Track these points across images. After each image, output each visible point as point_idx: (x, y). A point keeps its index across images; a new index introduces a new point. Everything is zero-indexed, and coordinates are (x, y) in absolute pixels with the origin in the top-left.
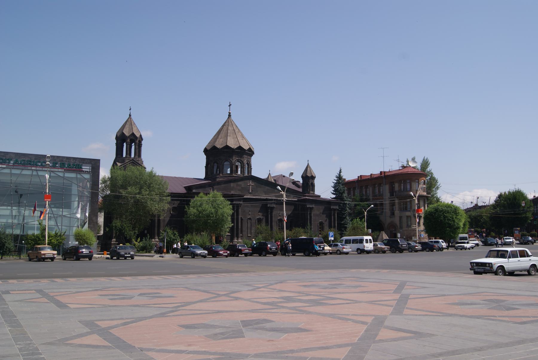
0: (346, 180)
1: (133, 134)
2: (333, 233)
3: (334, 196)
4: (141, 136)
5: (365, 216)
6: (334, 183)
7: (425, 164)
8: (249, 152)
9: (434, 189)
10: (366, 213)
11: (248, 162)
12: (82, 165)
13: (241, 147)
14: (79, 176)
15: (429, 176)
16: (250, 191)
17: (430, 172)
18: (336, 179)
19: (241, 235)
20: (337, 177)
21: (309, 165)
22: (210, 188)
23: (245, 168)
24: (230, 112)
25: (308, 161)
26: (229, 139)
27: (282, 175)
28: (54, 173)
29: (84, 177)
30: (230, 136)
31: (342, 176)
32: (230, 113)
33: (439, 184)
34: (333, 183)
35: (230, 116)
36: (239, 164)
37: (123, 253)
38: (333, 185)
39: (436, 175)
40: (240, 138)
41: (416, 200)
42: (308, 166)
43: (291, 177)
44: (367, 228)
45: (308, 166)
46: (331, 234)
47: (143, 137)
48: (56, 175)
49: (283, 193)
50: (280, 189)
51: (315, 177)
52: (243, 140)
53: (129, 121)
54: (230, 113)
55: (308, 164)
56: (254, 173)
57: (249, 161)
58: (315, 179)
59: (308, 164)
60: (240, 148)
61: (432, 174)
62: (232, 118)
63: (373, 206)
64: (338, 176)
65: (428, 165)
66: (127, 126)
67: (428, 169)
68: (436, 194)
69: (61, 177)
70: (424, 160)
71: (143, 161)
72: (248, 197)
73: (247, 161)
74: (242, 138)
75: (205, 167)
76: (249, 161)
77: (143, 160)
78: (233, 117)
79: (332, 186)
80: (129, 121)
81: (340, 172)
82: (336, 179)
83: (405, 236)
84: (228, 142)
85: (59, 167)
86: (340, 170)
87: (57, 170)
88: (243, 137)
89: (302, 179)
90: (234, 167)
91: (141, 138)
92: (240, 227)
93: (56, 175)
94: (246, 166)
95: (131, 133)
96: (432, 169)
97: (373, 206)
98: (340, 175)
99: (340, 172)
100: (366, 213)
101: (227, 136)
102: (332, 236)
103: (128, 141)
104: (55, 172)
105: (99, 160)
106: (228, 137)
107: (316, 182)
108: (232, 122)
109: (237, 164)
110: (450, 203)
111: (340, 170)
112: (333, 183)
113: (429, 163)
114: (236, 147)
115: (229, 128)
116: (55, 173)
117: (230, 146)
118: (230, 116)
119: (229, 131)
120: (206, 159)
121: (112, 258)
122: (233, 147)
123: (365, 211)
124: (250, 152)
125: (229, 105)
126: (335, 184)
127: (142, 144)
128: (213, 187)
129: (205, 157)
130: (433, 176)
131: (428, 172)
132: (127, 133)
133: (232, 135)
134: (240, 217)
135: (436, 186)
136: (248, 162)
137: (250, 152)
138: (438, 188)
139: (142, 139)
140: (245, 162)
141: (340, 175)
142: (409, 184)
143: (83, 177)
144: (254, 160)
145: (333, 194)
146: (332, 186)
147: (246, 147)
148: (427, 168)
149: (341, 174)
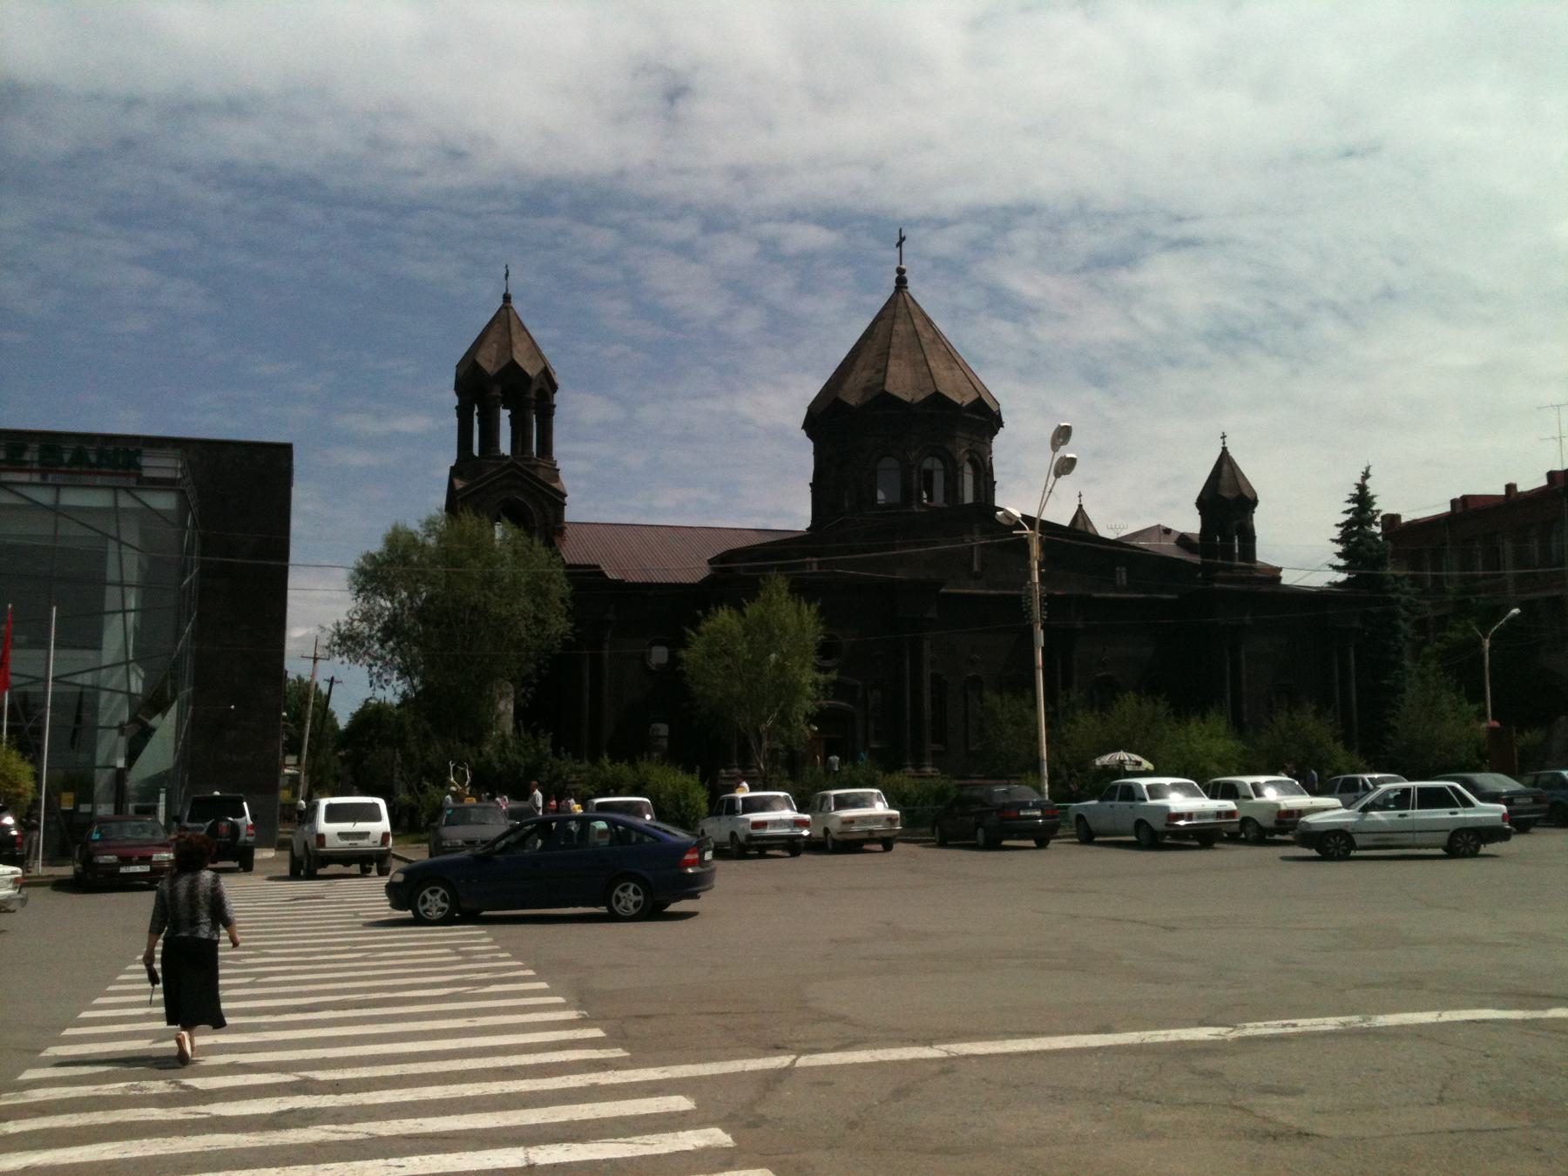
0: (1404, 520)
1: (513, 366)
3: (1341, 577)
4: (546, 373)
10: (1487, 643)
11: (976, 456)
14: (125, 501)
16: (976, 568)
19: (938, 747)
21: (1227, 453)
23: (960, 478)
24: (903, 266)
25: (1224, 437)
26: (894, 367)
27: (1159, 526)
28: (12, 491)
29: (148, 506)
30: (899, 357)
32: (901, 271)
35: (901, 282)
36: (938, 464)
37: (112, 858)
38: (1336, 533)
40: (938, 366)
42: (1225, 459)
43: (1062, 448)
45: (1225, 459)
47: (558, 379)
48: (28, 503)
49: (1028, 531)
52: (952, 368)
53: (504, 321)
54: (901, 271)
55: (1224, 449)
57: (980, 456)
58: (1257, 509)
59: (1224, 449)
60: (938, 401)
62: (909, 290)
63: (1516, 611)
66: (492, 336)
71: (558, 470)
72: (967, 591)
75: (811, 484)
76: (980, 456)
77: (557, 467)
78: (913, 287)
80: (504, 321)
84: (889, 381)
85: (36, 466)
87: (24, 477)
89: (1198, 511)
90: (915, 477)
91: (548, 384)
93: (22, 502)
94: (968, 469)
95: (504, 362)
97: (1516, 611)
98: (1362, 488)
101: (885, 355)
103: (494, 393)
104: (11, 487)
105: (285, 451)
106: (889, 362)
107: (1262, 521)
108: (911, 305)
109: (927, 464)
114: (921, 397)
115: (896, 328)
117: (896, 393)
118: (901, 282)
119: (894, 340)
120: (814, 453)
122: (907, 398)
123: (1485, 637)
125: (898, 240)
127: (554, 406)
132: (489, 362)
134: (927, 672)
136: (976, 456)
139: (554, 388)
140: (962, 454)
141: (1362, 488)
145: (1337, 568)
147: (964, 398)
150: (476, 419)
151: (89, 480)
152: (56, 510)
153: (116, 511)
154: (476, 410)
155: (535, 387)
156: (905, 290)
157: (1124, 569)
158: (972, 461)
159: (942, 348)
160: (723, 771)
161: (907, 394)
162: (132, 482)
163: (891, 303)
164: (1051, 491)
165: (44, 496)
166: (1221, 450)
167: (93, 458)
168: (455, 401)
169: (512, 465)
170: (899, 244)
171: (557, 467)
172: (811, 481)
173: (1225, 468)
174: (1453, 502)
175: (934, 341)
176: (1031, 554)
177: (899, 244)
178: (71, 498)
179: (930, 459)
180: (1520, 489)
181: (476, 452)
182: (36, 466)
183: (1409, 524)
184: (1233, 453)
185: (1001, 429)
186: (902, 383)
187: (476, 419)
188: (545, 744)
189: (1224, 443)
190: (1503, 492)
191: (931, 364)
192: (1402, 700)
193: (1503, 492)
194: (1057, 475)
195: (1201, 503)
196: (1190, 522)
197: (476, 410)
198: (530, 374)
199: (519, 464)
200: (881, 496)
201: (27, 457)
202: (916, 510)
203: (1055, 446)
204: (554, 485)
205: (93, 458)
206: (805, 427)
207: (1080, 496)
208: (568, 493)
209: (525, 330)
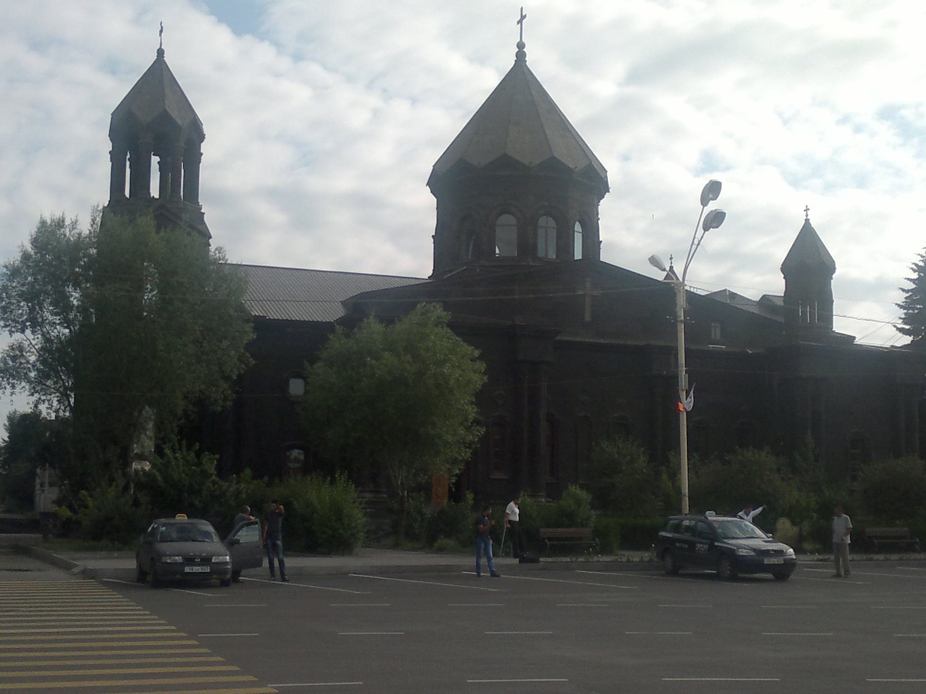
3: (907, 340)
6: (907, 291)
13: (559, 162)
18: (915, 276)
25: (807, 210)
32: (521, 46)
34: (903, 290)
35: (521, 56)
36: (552, 223)
54: (521, 46)
55: (807, 220)
59: (807, 220)
71: (204, 213)
77: (202, 211)
79: (899, 305)
82: (915, 276)
112: (903, 290)
125: (519, 18)
139: (202, 137)
145: (901, 330)
146: (899, 305)
150: (128, 163)
154: (128, 156)
164: (699, 244)
166: (804, 222)
170: (520, 22)
171: (202, 211)
172: (434, 234)
176: (678, 302)
177: (520, 22)
181: (127, 194)
185: (607, 194)
187: (128, 163)
188: (210, 464)
189: (807, 216)
194: (706, 228)
196: (776, 285)
197: (128, 156)
198: (180, 122)
200: (497, 251)
203: (704, 201)
204: (199, 227)
207: (671, 259)
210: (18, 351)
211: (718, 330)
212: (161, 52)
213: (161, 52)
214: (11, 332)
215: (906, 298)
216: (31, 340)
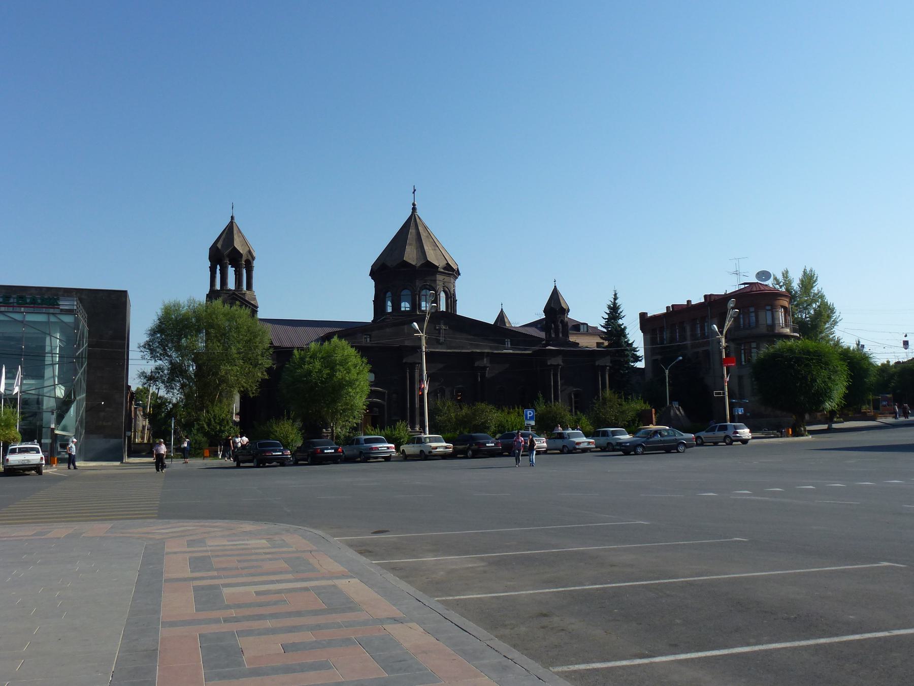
2: (532, 411)
4: (250, 252)
5: (665, 377)
6: (605, 319)
7: (808, 281)
8: (447, 272)
9: (827, 326)
10: (667, 372)
11: (446, 289)
12: (58, 299)
13: (429, 261)
14: (53, 319)
15: (818, 302)
17: (820, 294)
20: (609, 307)
22: (366, 336)
28: (4, 314)
30: (411, 244)
31: (619, 306)
32: (414, 205)
33: (837, 314)
34: (604, 318)
35: (414, 209)
39: (830, 299)
40: (428, 248)
41: (723, 340)
44: (671, 400)
46: (530, 414)
47: (255, 254)
48: (11, 319)
49: (421, 334)
50: (417, 327)
51: (568, 310)
54: (414, 205)
55: (555, 286)
56: (464, 310)
59: (555, 286)
61: (822, 297)
63: (681, 358)
64: (612, 306)
65: (815, 282)
67: (815, 290)
68: (834, 333)
69: (19, 321)
70: (805, 272)
73: (443, 286)
74: (433, 248)
81: (615, 299)
83: (749, 412)
86: (615, 295)
88: (435, 245)
92: (417, 406)
93: (11, 319)
94: (443, 295)
96: (822, 289)
97: (681, 358)
98: (615, 304)
99: (615, 299)
100: (667, 372)
102: (531, 418)
104: (6, 314)
105: (125, 292)
108: (418, 220)
110: (853, 346)
111: (615, 295)
112: (604, 318)
113: (817, 279)
116: (6, 315)
118: (414, 209)
120: (375, 287)
121: (238, 466)
122: (414, 263)
124: (452, 272)
125: (413, 191)
126: (607, 320)
128: (370, 335)
129: (372, 283)
130: (826, 301)
131: (815, 294)
133: (414, 242)
135: (832, 320)
136: (446, 289)
137: (452, 272)
138: (835, 323)
139: (253, 258)
140: (440, 287)
141: (615, 304)
142: (753, 314)
143: (60, 319)
144: (461, 287)
148: (812, 287)
149: (616, 302)
151: (37, 310)
152: (23, 323)
153: (48, 323)
155: (244, 258)
156: (415, 213)
157: (509, 340)
158: (444, 291)
159: (431, 240)
160: (324, 430)
161: (414, 261)
162: (57, 311)
163: (410, 218)
165: (18, 317)
167: (39, 301)
168: (209, 264)
169: (234, 294)
170: (414, 193)
173: (555, 295)
174: (668, 308)
175: (427, 237)
177: (414, 193)
178: (30, 318)
179: (425, 290)
180: (693, 303)
182: (15, 305)
183: (651, 317)
184: (558, 288)
186: (410, 255)
190: (703, 300)
191: (426, 248)
192: (621, 398)
193: (703, 300)
195: (545, 311)
199: (236, 293)
201: (12, 300)
202: (418, 313)
205: (39, 301)
206: (370, 275)
208: (259, 306)
209: (240, 232)
210: (159, 369)
211: (509, 343)
212: (232, 218)
213: (232, 218)
214: (155, 361)
215: (606, 322)
216: (164, 363)
